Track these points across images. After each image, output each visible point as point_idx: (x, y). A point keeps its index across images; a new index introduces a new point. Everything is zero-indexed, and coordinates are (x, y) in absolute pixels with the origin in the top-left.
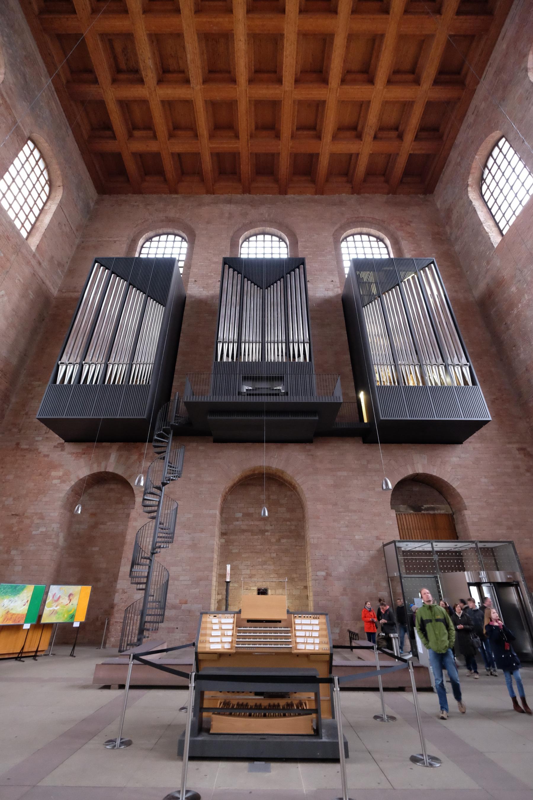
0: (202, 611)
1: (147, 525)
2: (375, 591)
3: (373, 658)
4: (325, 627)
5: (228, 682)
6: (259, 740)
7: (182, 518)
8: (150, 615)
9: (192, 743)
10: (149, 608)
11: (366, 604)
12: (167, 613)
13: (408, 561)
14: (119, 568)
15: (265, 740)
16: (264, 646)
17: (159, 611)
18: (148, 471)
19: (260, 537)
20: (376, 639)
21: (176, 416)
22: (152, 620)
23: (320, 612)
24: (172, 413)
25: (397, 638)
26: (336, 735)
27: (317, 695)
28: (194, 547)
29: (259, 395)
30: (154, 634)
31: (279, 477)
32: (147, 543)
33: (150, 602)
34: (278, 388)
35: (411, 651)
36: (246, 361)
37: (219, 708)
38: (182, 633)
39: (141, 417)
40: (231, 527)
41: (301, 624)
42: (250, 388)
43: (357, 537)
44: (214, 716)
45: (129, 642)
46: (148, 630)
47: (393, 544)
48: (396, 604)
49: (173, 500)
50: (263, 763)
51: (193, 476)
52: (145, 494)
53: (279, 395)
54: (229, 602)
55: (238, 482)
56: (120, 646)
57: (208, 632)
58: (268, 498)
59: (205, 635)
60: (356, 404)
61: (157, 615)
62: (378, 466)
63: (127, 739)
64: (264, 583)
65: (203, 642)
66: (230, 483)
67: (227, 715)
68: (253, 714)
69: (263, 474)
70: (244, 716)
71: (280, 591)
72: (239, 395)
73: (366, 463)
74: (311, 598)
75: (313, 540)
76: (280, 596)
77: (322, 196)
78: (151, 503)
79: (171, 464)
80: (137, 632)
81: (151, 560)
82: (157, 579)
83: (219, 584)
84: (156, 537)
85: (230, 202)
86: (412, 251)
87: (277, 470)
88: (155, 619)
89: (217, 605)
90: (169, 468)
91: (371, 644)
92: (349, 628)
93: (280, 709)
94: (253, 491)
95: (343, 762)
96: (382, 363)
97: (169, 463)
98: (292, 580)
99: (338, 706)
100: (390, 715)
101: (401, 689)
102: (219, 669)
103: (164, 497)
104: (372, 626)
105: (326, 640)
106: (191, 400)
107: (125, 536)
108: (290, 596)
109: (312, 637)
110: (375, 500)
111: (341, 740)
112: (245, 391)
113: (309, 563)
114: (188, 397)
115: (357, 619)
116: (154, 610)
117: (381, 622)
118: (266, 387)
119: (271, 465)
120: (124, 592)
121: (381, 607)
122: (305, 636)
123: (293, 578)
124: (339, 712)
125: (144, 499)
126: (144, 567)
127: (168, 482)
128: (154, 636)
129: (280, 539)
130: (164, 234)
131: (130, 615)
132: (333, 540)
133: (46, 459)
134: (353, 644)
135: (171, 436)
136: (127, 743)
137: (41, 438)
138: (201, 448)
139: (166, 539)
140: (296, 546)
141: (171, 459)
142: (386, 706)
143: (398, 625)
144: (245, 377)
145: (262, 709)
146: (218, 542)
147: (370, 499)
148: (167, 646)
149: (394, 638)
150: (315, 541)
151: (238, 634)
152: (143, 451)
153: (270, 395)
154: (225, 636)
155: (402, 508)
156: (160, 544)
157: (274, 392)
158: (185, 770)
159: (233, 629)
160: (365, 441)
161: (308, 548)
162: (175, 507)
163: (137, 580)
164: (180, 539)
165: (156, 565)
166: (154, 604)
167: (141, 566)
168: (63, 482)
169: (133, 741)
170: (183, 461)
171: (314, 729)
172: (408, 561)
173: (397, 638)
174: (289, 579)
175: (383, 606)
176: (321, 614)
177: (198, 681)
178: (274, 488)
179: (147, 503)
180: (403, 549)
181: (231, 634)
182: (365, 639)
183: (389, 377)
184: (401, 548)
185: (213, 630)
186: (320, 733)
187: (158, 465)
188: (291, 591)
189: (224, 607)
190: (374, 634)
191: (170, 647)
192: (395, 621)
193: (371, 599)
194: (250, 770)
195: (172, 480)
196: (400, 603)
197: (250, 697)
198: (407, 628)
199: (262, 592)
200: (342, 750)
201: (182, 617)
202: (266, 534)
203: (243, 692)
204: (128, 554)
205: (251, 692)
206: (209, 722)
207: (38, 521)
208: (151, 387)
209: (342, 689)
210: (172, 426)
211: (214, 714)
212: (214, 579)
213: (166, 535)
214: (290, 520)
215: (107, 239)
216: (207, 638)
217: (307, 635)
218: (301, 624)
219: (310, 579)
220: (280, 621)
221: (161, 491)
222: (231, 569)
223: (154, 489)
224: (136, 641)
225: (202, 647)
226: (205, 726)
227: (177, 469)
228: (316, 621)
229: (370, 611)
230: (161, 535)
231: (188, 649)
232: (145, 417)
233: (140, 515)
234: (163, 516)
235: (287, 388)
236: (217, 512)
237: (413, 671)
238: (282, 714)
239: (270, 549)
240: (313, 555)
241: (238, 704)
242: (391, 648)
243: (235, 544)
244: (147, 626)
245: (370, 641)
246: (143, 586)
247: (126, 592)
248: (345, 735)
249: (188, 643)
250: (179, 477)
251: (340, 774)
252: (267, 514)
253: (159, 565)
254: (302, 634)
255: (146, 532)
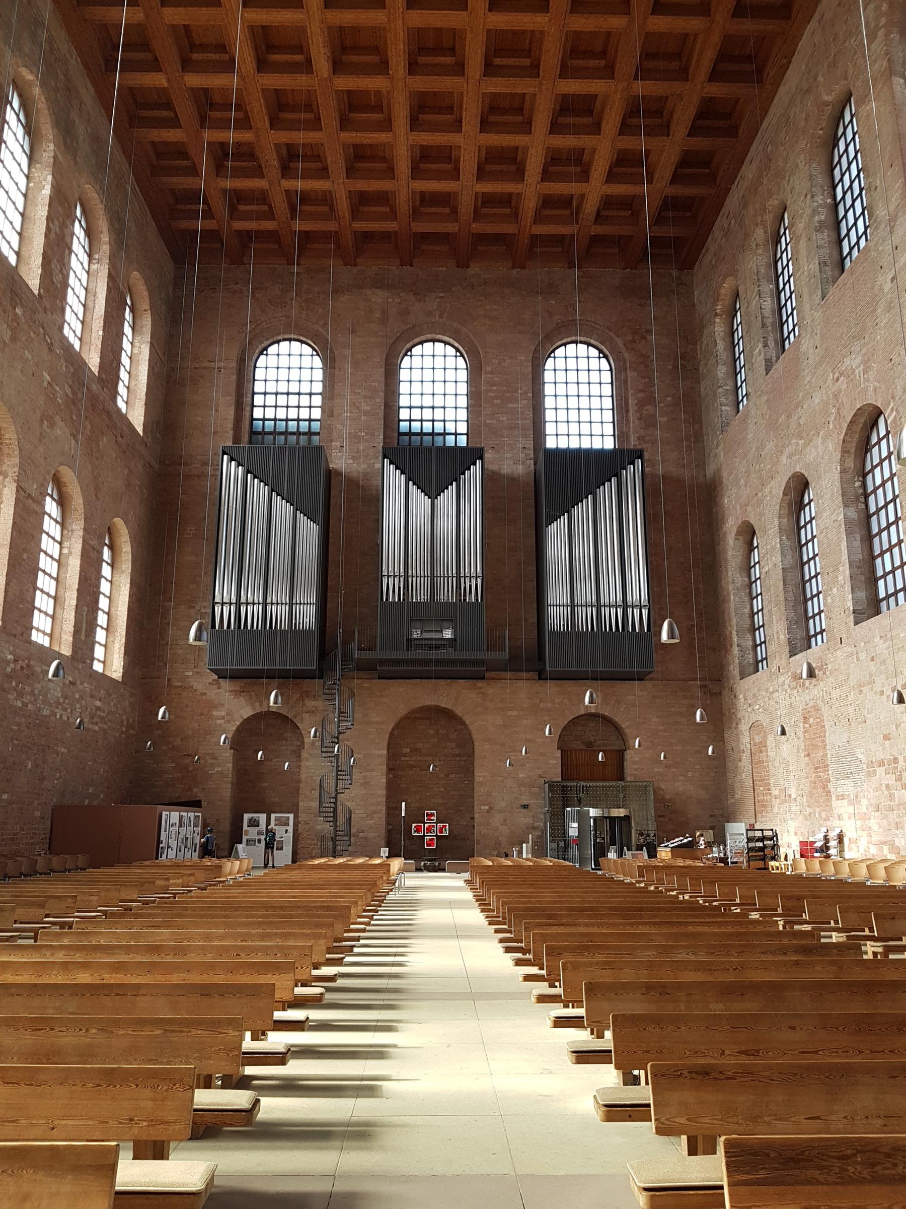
77: (524, 272)
85: (379, 283)
86: (641, 391)
130: (284, 340)
133: (204, 697)
137: (191, 673)
168: (228, 722)
207: (212, 761)
214: (458, 755)
215: (207, 364)
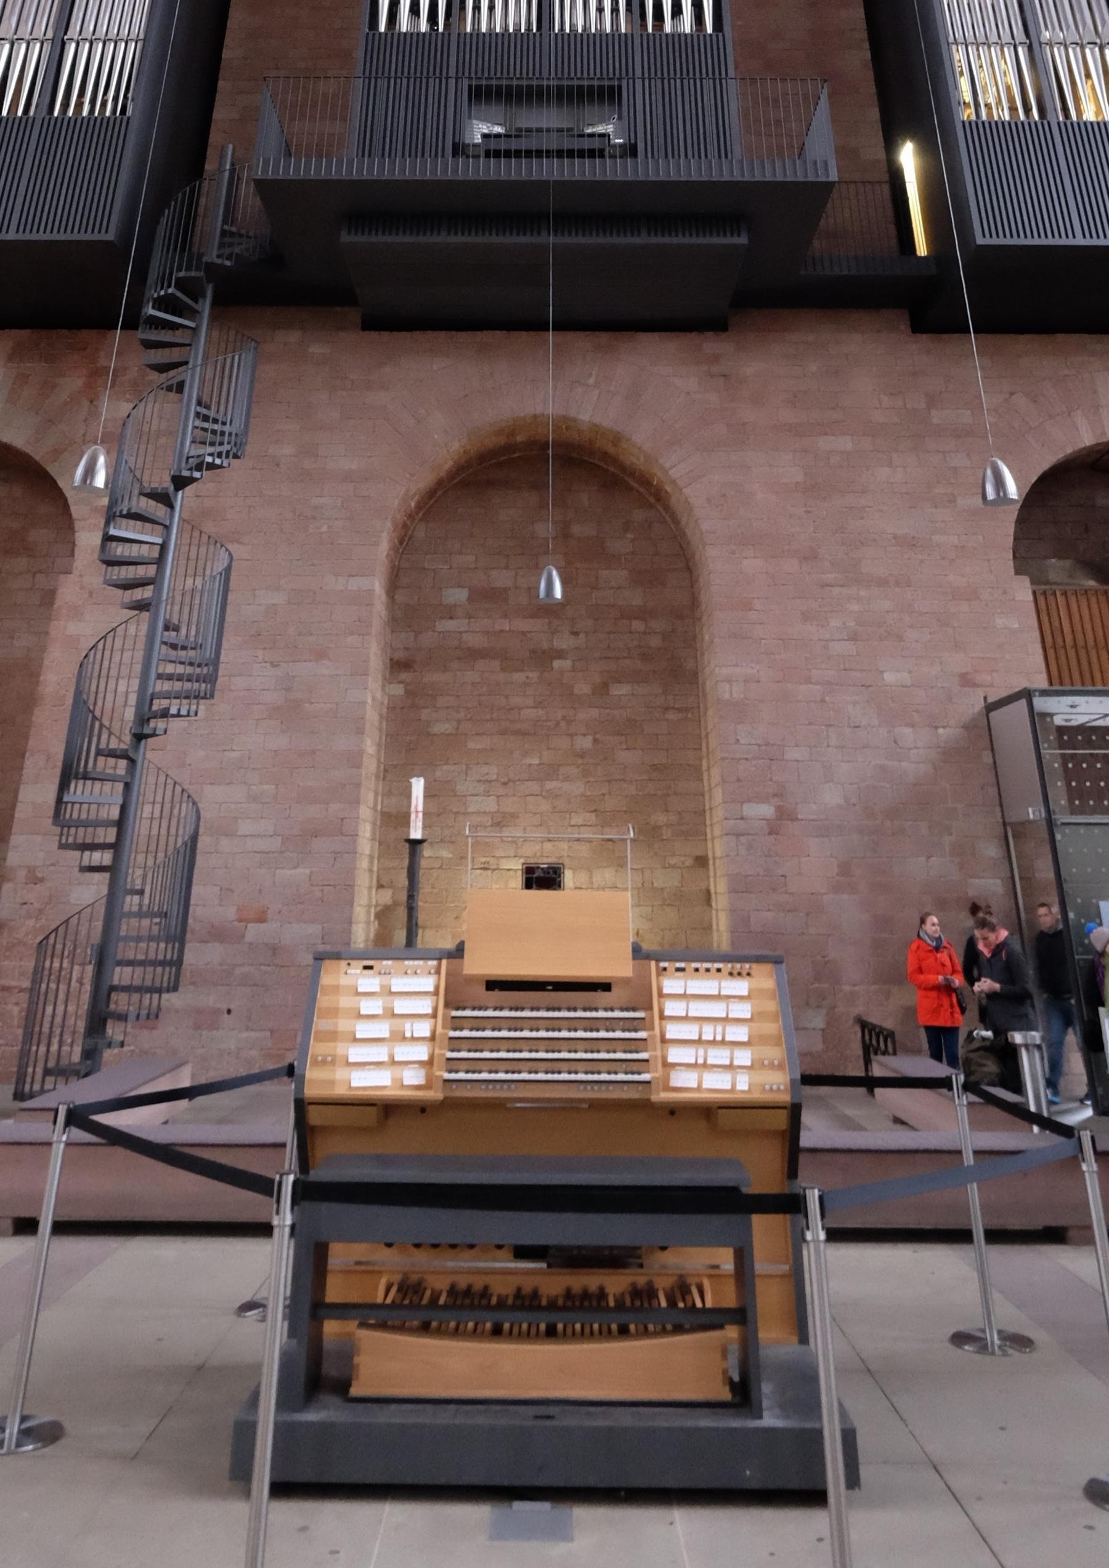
0: (321, 948)
1: (120, 631)
2: (954, 876)
3: (949, 1122)
4: (771, 1006)
5: (416, 1209)
6: (530, 1423)
7: (244, 607)
8: (130, 963)
9: (282, 1432)
10: (126, 939)
11: (923, 921)
12: (195, 956)
13: (1078, 764)
14: (16, 792)
15: (554, 1423)
16: (550, 1077)
17: (161, 950)
18: (122, 436)
19: (534, 675)
20: (961, 1052)
21: (224, 233)
22: (137, 982)
23: (755, 952)
24: (212, 221)
25: (1039, 1047)
26: (810, 1404)
27: (743, 1257)
28: (290, 712)
29: (529, 154)
30: (146, 1033)
31: (605, 456)
32: (120, 700)
33: (130, 915)
34: (600, 129)
35: (1087, 1097)
36: (484, 29)
37: (382, 1306)
38: (248, 1029)
39: (96, 237)
40: (427, 639)
41: (684, 996)
42: (498, 129)
43: (889, 677)
44: (364, 1334)
45: (51, 1064)
46: (122, 1018)
47: (1023, 702)
48: (1032, 923)
49: (215, 541)
50: (544, 1506)
51: (287, 450)
52: (111, 517)
53: (602, 155)
54: (422, 917)
55: (452, 475)
56: (21, 1079)
57: (343, 1025)
58: (564, 534)
59: (333, 1036)
60: (886, 188)
61: (154, 963)
62: (966, 417)
63: (43, 1417)
64: (548, 846)
65: (324, 1062)
66: (424, 480)
67: (412, 1331)
68: (507, 1326)
69: (546, 445)
70: (476, 1334)
71: (607, 875)
72: (455, 154)
73: (923, 405)
74: (721, 902)
75: (727, 686)
76: (609, 893)
78: (133, 551)
79: (208, 407)
80: (81, 1025)
81: (132, 762)
82: (155, 832)
83: (384, 848)
84: (153, 676)
87: (596, 429)
88: (149, 977)
89: (374, 926)
90: (198, 423)
91: (940, 1070)
92: (858, 1009)
93: (608, 1309)
94: (509, 509)
95: (838, 1503)
96: (981, 38)
97: (199, 403)
98: (649, 835)
99: (821, 1297)
100: (1012, 1329)
101: (1054, 1235)
102: (383, 1160)
103: (180, 531)
104: (946, 1001)
105: (775, 1053)
106: (281, 175)
107: (38, 675)
108: (646, 892)
109: (723, 1042)
110: (955, 540)
111: (831, 1421)
112: (478, 139)
113: (715, 772)
114: (268, 163)
115: (890, 977)
116: (143, 945)
117: (977, 987)
118: (555, 124)
119: (572, 413)
120: (35, 879)
121: (977, 933)
122: (699, 1042)
123: (656, 829)
124: (823, 1320)
125: (108, 538)
126: (108, 786)
127: (197, 475)
128: (143, 1039)
129: (605, 686)
131: (56, 965)
132: (803, 688)
134: (877, 1071)
135: (205, 307)
136: (47, 1434)
138: (317, 349)
139: (188, 685)
140: (667, 709)
141: (207, 390)
142: (996, 1296)
143: (1039, 999)
144: (479, 88)
145: (540, 1308)
146: (379, 695)
147: (937, 538)
148: (193, 1076)
149: (1027, 1046)
150: (737, 692)
151: (452, 1034)
152: (102, 362)
153: (571, 154)
154: (404, 1039)
155: (1057, 569)
156: (165, 703)
157: (586, 144)
158: (257, 1531)
159: (434, 1016)
160: (922, 324)
161: (712, 719)
162: (220, 566)
163: (82, 835)
164: (239, 683)
165: (152, 780)
166: (146, 922)
167: (98, 784)
169: (67, 1425)
170: (250, 397)
171: (731, 1383)
172: (1078, 764)
173: (1039, 1047)
174: (639, 831)
175: (986, 932)
176: (759, 960)
177: (306, 1205)
178: (585, 497)
179: (120, 550)
180: (1058, 721)
181: (428, 1034)
182: (918, 1052)
183: (1008, 89)
184: (1051, 715)
185: (360, 1016)
186: (754, 1395)
187: (158, 411)
188: (647, 873)
189: (402, 933)
190: (953, 1031)
191: (203, 1080)
192: (1032, 986)
193: (941, 905)
194: (498, 1533)
195: (211, 466)
196: (1048, 917)
197: (498, 1265)
198: (1075, 1010)
199: (542, 878)
200: (834, 1459)
201: (246, 969)
202: (557, 664)
203: (472, 1247)
204: (48, 738)
205: (500, 1247)
206: (347, 1354)
208: (134, 125)
209: (836, 1235)
210: (210, 268)
211: (363, 1325)
212: (366, 831)
213: (189, 670)
214: (643, 614)
216: (341, 1048)
217: (708, 1036)
218: (684, 996)
219: (717, 831)
220: (606, 987)
221: (171, 506)
222: (428, 795)
223: (143, 499)
224: (76, 1057)
225: (318, 1082)
226: (330, 1369)
227: (227, 428)
228: (741, 987)
229: (937, 949)
230: (170, 669)
231: (268, 1087)
232: (110, 237)
233: (91, 594)
234: (178, 598)
235: (631, 130)
236: (378, 586)
237: (1095, 1167)
238: (614, 1327)
239: (569, 722)
240: (730, 742)
241: (453, 1291)
242: (1017, 1087)
243: (441, 701)
244: (120, 1002)
245: (940, 1060)
246: (103, 858)
247: (42, 880)
248: (847, 1404)
249: (270, 1066)
250: (236, 456)
251: (826, 1546)
252: (558, 593)
253: (162, 779)
254: (689, 1032)
255: (116, 658)
